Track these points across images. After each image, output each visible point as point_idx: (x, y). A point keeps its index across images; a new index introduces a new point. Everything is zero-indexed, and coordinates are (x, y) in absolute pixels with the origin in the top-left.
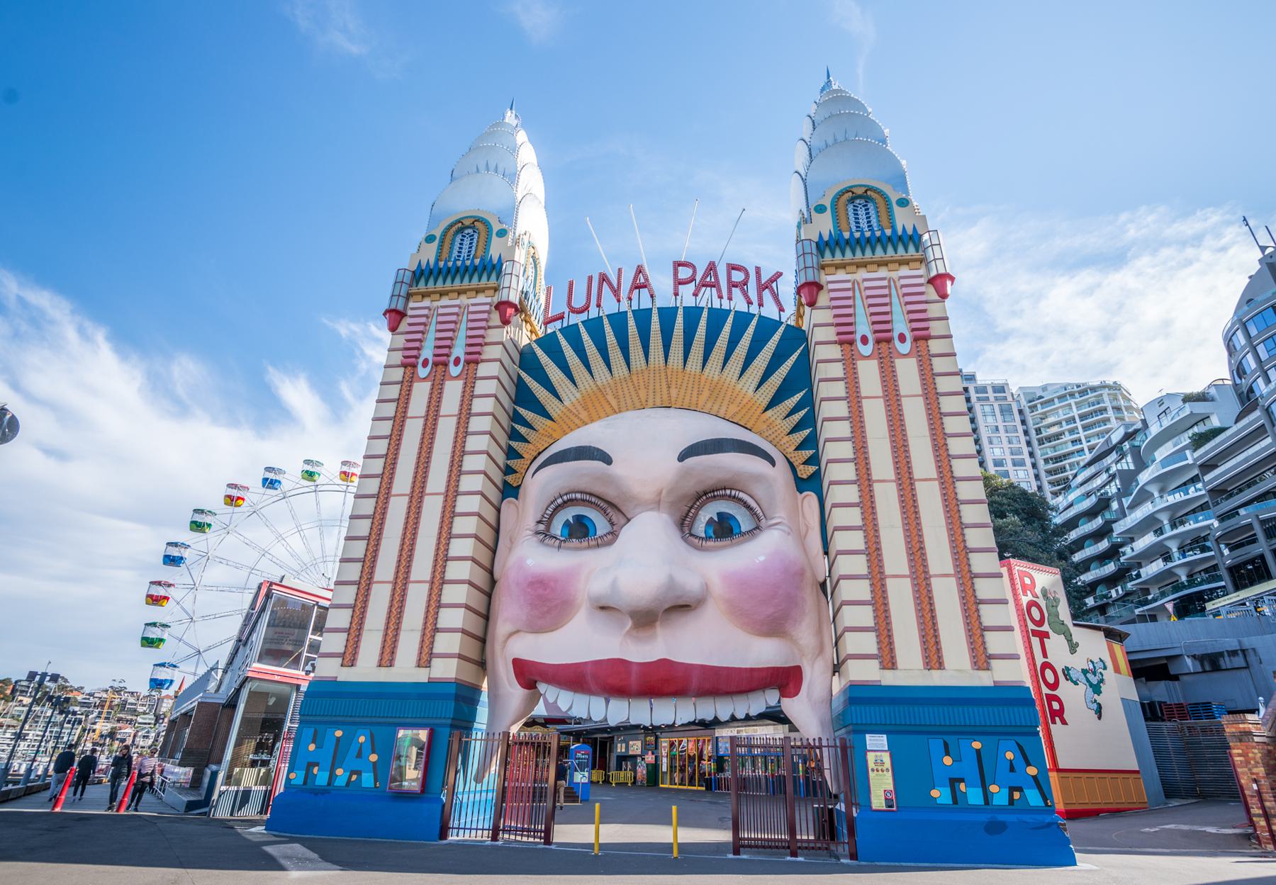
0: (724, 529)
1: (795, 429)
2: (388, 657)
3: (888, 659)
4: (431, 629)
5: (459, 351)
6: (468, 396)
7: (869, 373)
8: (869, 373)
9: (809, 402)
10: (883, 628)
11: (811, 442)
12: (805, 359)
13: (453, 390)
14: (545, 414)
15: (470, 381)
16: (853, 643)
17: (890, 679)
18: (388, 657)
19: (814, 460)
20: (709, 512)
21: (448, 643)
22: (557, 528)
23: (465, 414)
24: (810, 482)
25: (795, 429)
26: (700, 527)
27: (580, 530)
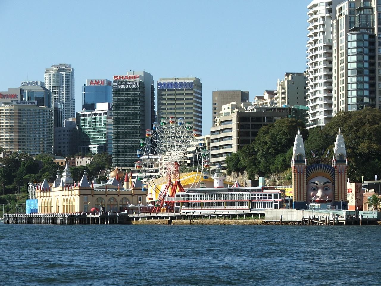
0: (326, 189)
1: (333, 179)
2: (300, 200)
3: (338, 200)
4: (303, 198)
5: (302, 171)
6: (303, 176)
7: (340, 175)
8: (340, 175)
9: (334, 176)
10: (338, 198)
11: (334, 180)
12: (334, 172)
13: (302, 175)
14: (309, 176)
15: (303, 174)
16: (336, 199)
17: (338, 201)
18: (300, 200)
19: (334, 182)
20: (326, 188)
21: (305, 199)
22: (312, 189)
23: (303, 178)
24: (334, 184)
25: (333, 179)
26: (325, 189)
27: (314, 189)
